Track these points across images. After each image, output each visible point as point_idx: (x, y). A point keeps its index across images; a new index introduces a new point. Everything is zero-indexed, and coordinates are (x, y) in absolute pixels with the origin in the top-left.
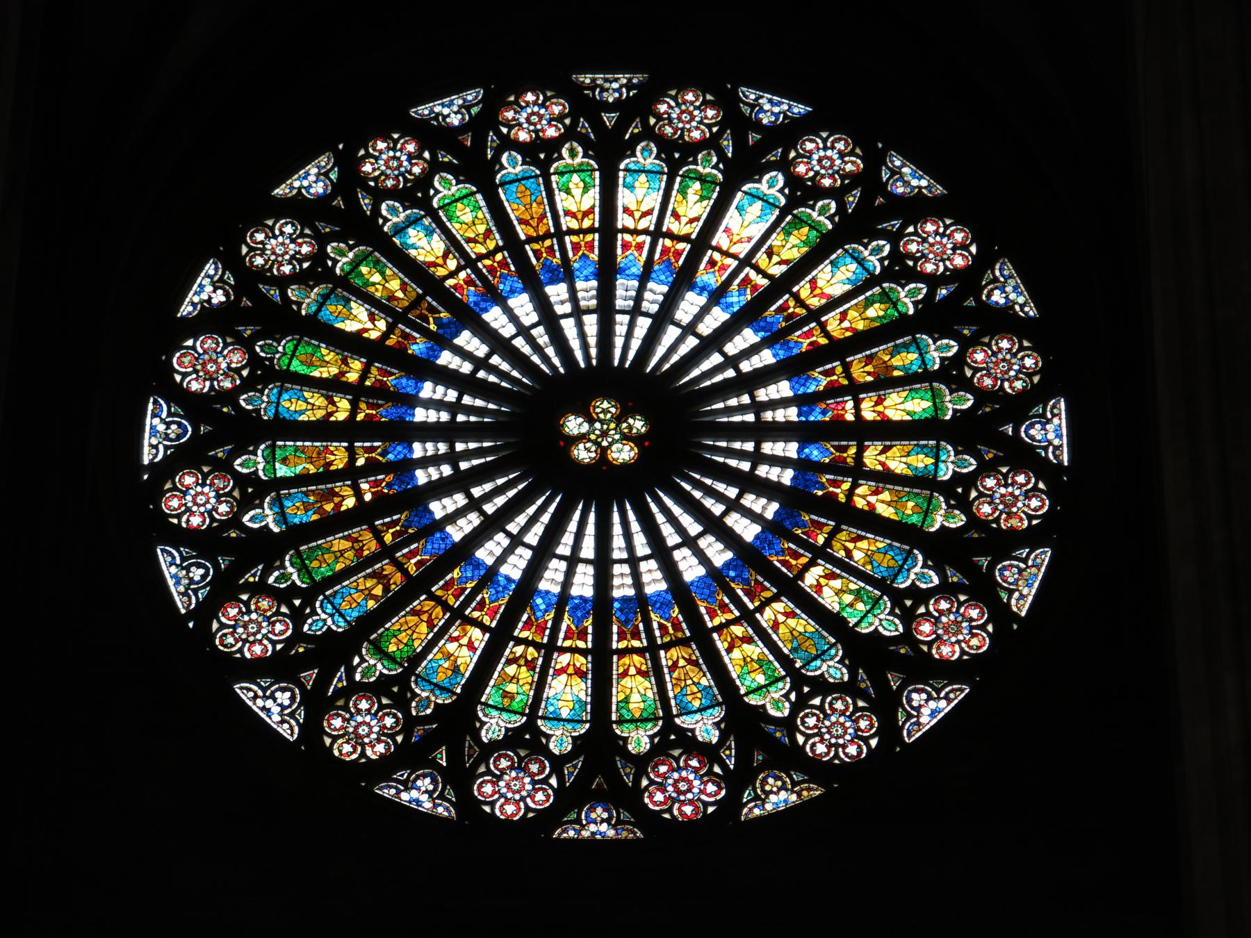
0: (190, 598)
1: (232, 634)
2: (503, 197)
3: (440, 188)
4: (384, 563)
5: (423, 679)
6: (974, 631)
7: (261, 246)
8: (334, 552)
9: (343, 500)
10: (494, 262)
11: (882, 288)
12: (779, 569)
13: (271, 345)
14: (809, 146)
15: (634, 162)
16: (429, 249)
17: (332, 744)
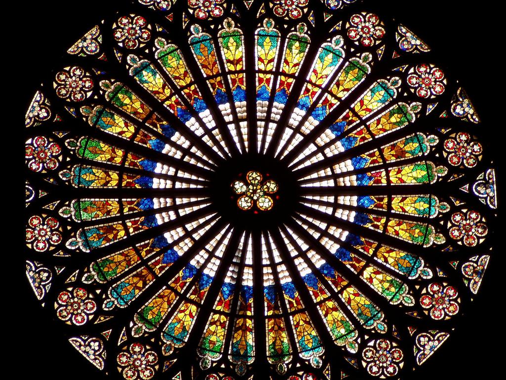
0: (41, 290)
1: (65, 310)
2: (193, 51)
3: (158, 47)
4: (142, 268)
5: (167, 334)
6: (451, 302)
7: (63, 83)
8: (116, 262)
9: (118, 232)
10: (190, 91)
11: (398, 105)
12: (349, 269)
13: (73, 142)
14: (357, 20)
15: (262, 30)
16: (154, 83)
17: (122, 371)
